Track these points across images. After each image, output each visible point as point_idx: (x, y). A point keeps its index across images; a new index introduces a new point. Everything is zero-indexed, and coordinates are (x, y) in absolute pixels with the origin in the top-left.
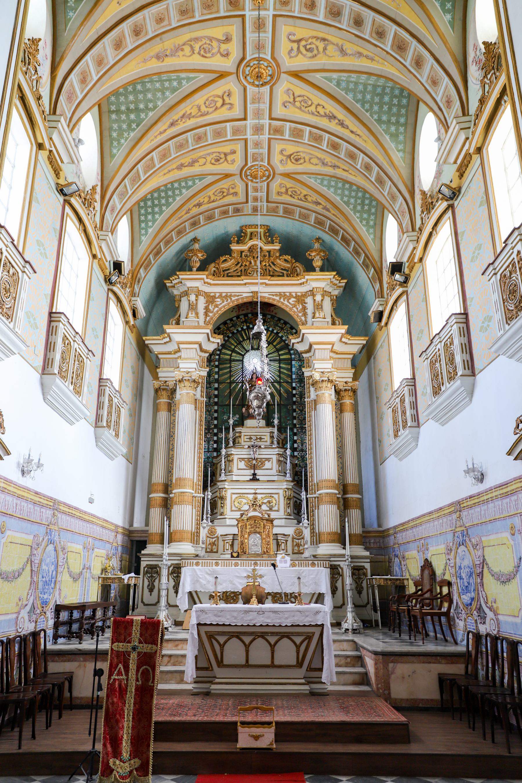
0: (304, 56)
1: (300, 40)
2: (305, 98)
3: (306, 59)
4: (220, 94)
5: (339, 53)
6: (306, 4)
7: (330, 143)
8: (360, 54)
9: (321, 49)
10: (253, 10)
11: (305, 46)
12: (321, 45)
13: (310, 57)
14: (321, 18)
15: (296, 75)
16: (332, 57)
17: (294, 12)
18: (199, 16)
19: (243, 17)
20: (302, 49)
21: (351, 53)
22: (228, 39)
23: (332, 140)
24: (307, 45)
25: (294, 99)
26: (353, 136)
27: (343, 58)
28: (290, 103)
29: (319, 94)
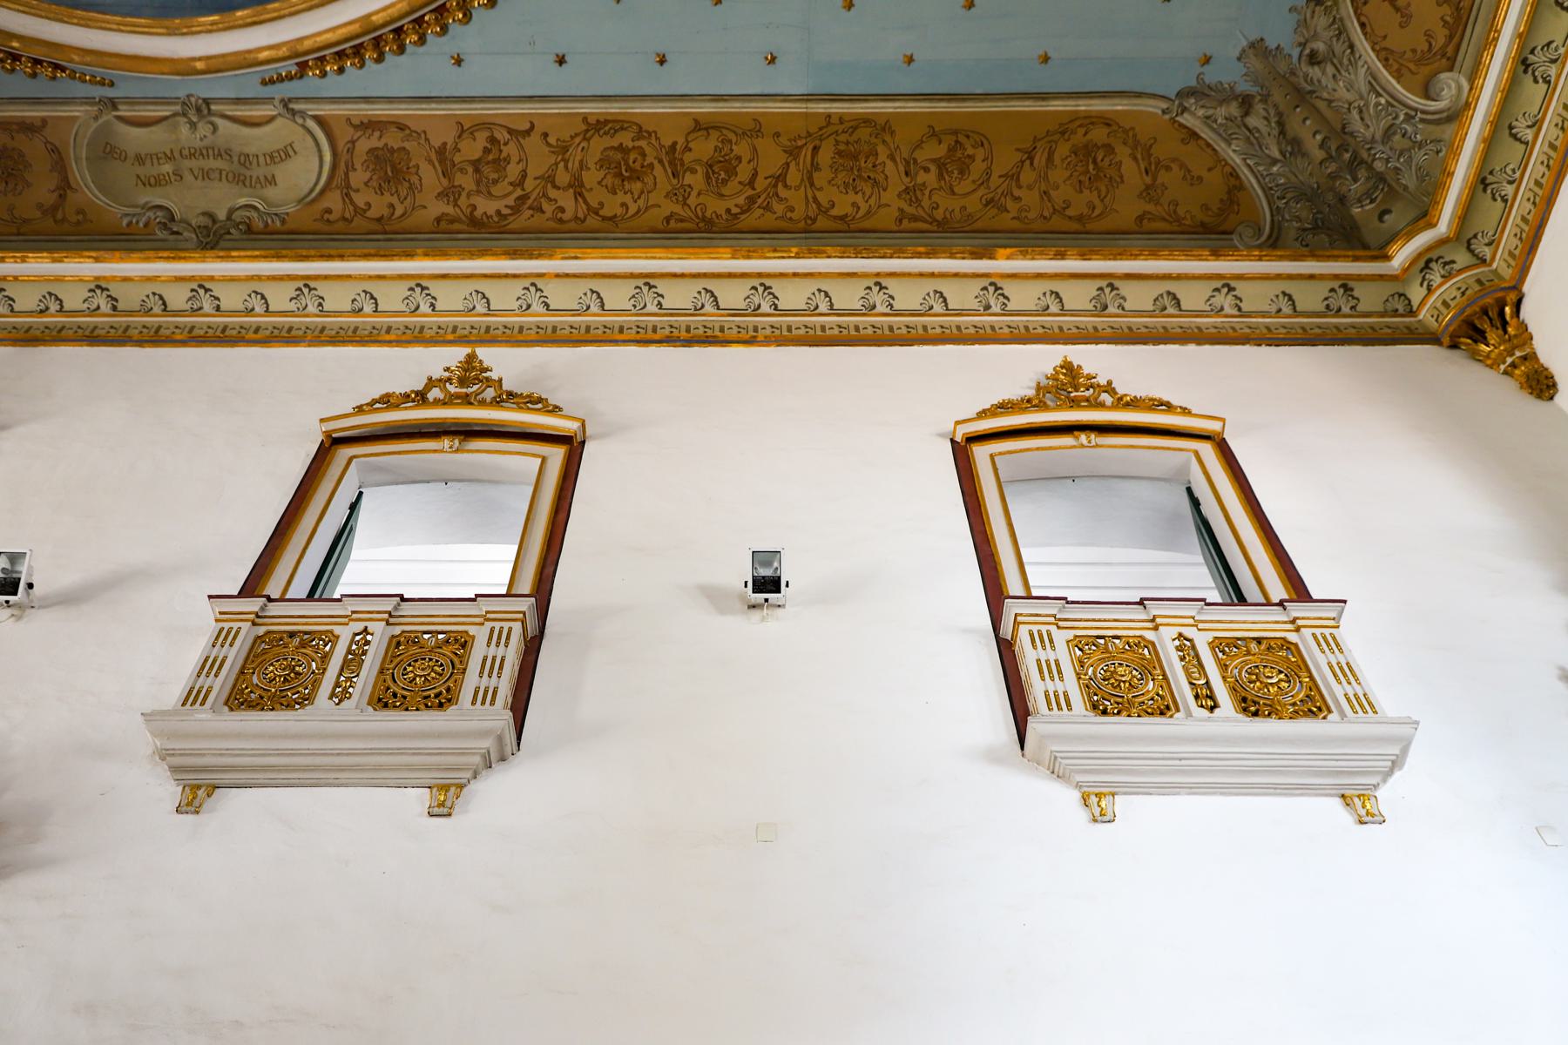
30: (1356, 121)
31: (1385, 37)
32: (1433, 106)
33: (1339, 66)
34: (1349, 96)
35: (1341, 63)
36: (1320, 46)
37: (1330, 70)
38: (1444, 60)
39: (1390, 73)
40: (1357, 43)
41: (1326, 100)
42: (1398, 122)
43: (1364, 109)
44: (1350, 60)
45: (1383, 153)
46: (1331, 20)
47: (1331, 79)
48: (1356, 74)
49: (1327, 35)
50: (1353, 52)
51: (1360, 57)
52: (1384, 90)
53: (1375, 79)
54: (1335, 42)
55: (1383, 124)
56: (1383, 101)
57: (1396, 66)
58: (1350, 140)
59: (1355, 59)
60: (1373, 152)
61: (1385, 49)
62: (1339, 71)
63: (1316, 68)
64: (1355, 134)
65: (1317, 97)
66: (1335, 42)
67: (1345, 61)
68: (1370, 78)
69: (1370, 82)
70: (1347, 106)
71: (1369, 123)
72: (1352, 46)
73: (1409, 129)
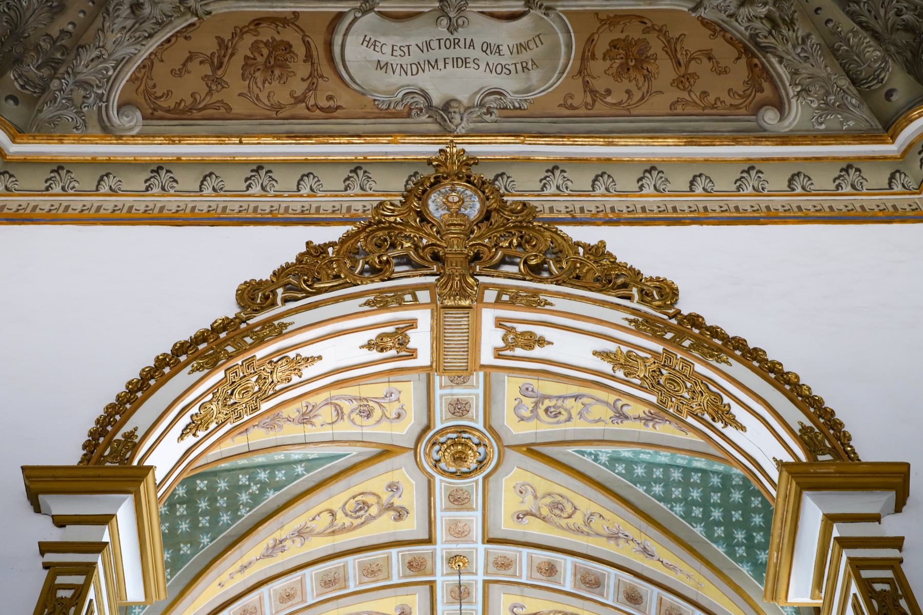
30: (90, 56)
31: (162, 61)
32: (113, 113)
33: (133, 30)
34: (110, 46)
35: (135, 31)
36: (147, 10)
37: (129, 23)
38: (150, 111)
39: (134, 72)
40: (154, 39)
41: (103, 26)
42: (95, 89)
43: (101, 59)
44: (139, 37)
45: (67, 85)
46: (170, 14)
47: (121, 26)
48: (128, 45)
49: (157, 12)
50: (146, 38)
51: (142, 45)
52: (119, 72)
53: (127, 62)
54: (152, 21)
55: (92, 79)
56: (110, 73)
57: (140, 75)
58: (73, 55)
59: (141, 41)
60: (66, 76)
61: (152, 63)
62: (129, 30)
63: (129, 11)
64: (78, 58)
65: (104, 18)
66: (152, 21)
67: (137, 34)
68: (127, 57)
69: (124, 58)
70: (101, 44)
71: (89, 67)
72: (151, 36)
73: (91, 100)
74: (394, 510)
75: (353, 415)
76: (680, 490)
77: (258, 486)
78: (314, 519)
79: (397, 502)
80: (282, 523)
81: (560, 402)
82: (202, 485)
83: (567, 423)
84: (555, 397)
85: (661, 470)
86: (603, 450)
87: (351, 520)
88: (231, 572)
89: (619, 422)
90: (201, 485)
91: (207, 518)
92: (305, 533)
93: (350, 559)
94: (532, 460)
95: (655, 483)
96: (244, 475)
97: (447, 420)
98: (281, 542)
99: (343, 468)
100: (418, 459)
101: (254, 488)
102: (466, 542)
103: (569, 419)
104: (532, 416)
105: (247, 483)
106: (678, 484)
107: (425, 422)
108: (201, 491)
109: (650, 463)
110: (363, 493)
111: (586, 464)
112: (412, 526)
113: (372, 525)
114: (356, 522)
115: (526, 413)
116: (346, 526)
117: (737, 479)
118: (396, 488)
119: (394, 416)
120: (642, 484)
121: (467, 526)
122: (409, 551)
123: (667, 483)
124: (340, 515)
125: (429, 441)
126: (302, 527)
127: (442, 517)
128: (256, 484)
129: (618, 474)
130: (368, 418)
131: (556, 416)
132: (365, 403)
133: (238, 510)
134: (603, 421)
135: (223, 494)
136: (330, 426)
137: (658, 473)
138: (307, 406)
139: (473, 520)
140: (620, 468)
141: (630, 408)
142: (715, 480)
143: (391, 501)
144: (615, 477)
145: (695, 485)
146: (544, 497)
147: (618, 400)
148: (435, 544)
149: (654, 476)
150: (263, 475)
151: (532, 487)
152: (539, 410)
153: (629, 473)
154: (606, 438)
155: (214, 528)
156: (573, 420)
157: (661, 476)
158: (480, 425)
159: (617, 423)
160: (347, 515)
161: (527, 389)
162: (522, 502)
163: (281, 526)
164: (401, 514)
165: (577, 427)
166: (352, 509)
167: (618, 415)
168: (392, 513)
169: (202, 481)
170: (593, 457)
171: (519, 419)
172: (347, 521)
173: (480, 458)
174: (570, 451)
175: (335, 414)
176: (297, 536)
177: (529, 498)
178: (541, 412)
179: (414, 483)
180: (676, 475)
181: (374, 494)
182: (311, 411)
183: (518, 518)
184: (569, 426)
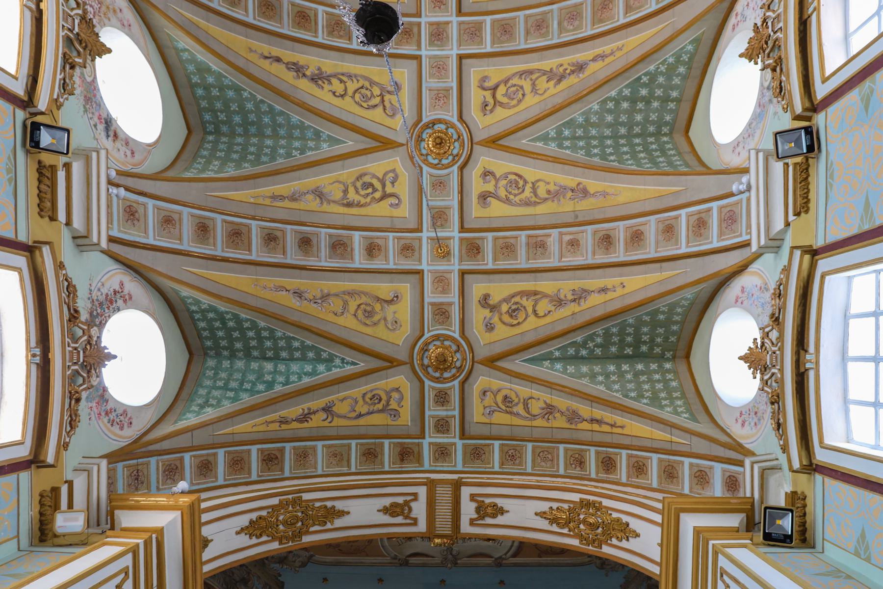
0: (374, 176)
1: (382, 198)
2: (365, 105)
3: (372, 170)
4: (499, 109)
5: (325, 191)
6: (379, 250)
7: (313, 23)
8: (293, 198)
9: (351, 190)
10: (449, 238)
11: (375, 190)
12: (352, 196)
13: (365, 174)
14: (357, 235)
15: (385, 144)
16: (334, 182)
17: (394, 238)
18: (520, 236)
19: (462, 229)
20: (378, 185)
21: (307, 196)
22: (484, 197)
23: (309, 31)
24: (372, 193)
25: (383, 101)
26: (276, 51)
27: (318, 185)
28: (389, 92)
29: (345, 117)
74: (490, 305)
75: (516, 400)
76: (280, 345)
77: (588, 346)
78: (549, 312)
79: (486, 312)
80: (573, 318)
81: (371, 409)
82: (629, 350)
83: (365, 392)
84: (375, 412)
85: (295, 357)
86: (338, 370)
87: (521, 302)
88: (614, 293)
89: (328, 404)
90: (629, 351)
91: (627, 332)
92: (556, 301)
93: (524, 266)
94: (389, 354)
95: (298, 348)
96: (597, 354)
97: (450, 388)
98: (574, 300)
99: (525, 351)
100: (471, 355)
101: (591, 345)
102: (436, 272)
103: (364, 395)
104: (390, 393)
105: (596, 349)
106: (282, 349)
107: (466, 386)
108: (629, 347)
109: (304, 360)
110: (513, 326)
111: (349, 355)
112: (478, 288)
113: (506, 293)
114: (517, 299)
115: (395, 395)
116: (526, 297)
117: (240, 355)
118: (488, 327)
119: (488, 394)
120: (308, 346)
121: (435, 287)
122: (479, 265)
123: (290, 348)
124: (530, 310)
125: (463, 371)
126: (558, 308)
127: (453, 297)
128: (589, 347)
129: (326, 351)
130: (506, 395)
131: (374, 396)
132: (508, 409)
133: (604, 333)
134: (340, 400)
135: (614, 344)
136: (534, 396)
137: (297, 354)
138: (548, 419)
139: (431, 294)
140: (325, 355)
141: (322, 419)
142: (255, 353)
143: (492, 314)
144: (328, 349)
145: (270, 349)
146: (379, 320)
147: (330, 422)
148: (459, 269)
149: (300, 352)
150: (584, 352)
151: (388, 328)
152: (386, 399)
153: (318, 352)
154: (336, 387)
155: (623, 326)
156: (361, 395)
157: (295, 352)
158: (427, 383)
159: (330, 402)
160: (525, 308)
161: (395, 416)
162: (395, 313)
163: (573, 316)
164: (485, 301)
165: (357, 391)
166: (520, 312)
167: (330, 409)
168: (491, 302)
169: (628, 353)
170: (345, 361)
171: (399, 389)
172: (524, 302)
173: (427, 353)
174: (362, 364)
175: (529, 406)
176: (563, 301)
177: (390, 318)
178: (384, 397)
179: (474, 330)
180: (284, 354)
181: (504, 323)
182: (546, 414)
183: (397, 297)
184: (364, 389)
